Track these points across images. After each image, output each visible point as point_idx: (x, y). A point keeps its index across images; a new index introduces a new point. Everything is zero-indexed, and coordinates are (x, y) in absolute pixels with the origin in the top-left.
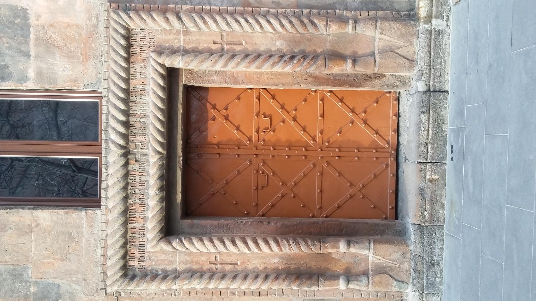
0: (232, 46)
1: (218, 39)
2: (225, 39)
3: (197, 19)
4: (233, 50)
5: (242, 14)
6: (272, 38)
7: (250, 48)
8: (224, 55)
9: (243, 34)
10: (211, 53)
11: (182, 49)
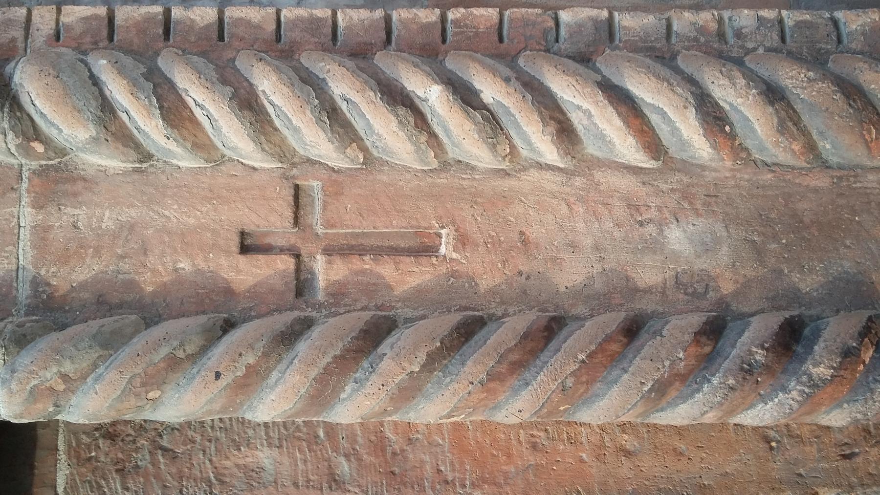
0: (367, 263)
1: (273, 220)
2: (316, 218)
3: (118, 90)
4: (374, 287)
5: (431, 52)
6: (633, 207)
7: (488, 274)
8: (307, 324)
9: (442, 180)
10: (220, 315)
11: (24, 292)
